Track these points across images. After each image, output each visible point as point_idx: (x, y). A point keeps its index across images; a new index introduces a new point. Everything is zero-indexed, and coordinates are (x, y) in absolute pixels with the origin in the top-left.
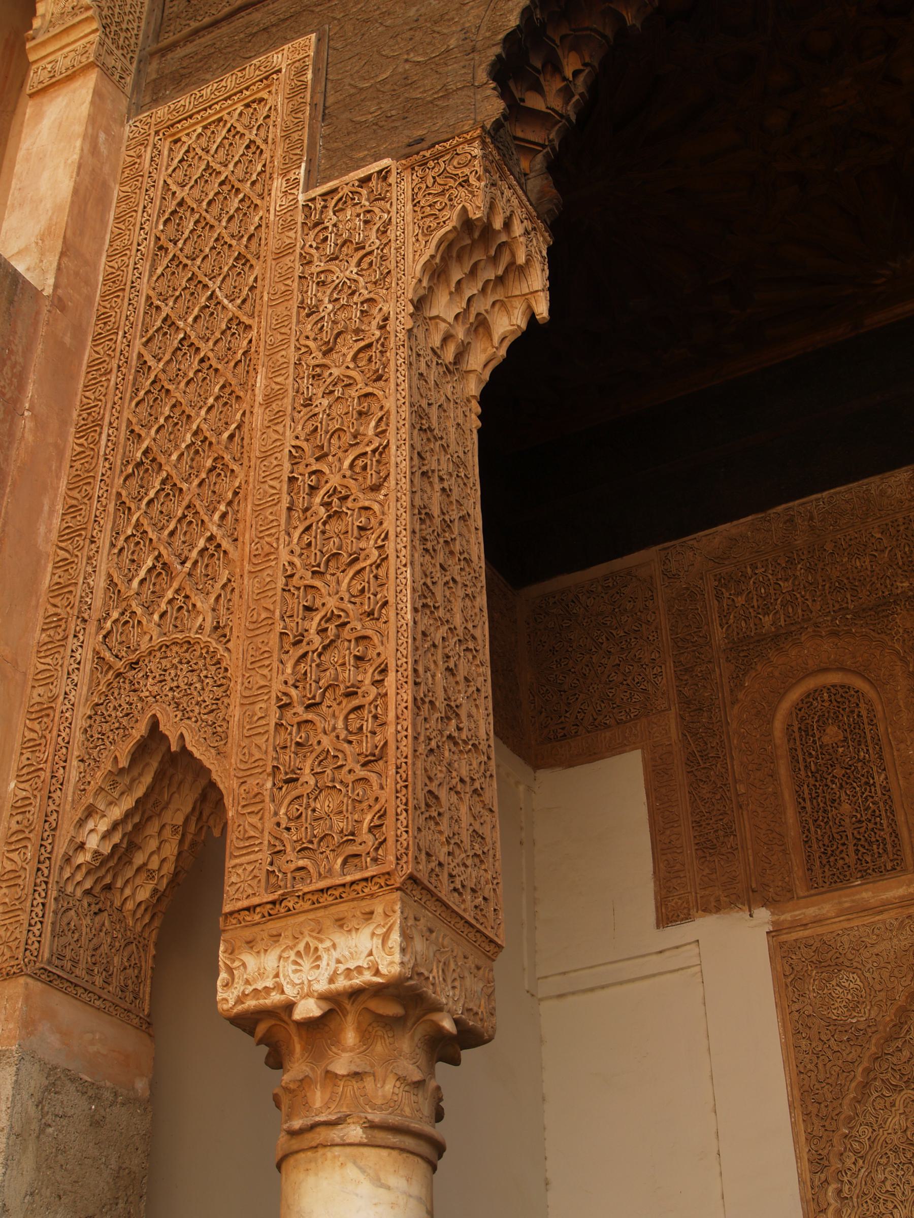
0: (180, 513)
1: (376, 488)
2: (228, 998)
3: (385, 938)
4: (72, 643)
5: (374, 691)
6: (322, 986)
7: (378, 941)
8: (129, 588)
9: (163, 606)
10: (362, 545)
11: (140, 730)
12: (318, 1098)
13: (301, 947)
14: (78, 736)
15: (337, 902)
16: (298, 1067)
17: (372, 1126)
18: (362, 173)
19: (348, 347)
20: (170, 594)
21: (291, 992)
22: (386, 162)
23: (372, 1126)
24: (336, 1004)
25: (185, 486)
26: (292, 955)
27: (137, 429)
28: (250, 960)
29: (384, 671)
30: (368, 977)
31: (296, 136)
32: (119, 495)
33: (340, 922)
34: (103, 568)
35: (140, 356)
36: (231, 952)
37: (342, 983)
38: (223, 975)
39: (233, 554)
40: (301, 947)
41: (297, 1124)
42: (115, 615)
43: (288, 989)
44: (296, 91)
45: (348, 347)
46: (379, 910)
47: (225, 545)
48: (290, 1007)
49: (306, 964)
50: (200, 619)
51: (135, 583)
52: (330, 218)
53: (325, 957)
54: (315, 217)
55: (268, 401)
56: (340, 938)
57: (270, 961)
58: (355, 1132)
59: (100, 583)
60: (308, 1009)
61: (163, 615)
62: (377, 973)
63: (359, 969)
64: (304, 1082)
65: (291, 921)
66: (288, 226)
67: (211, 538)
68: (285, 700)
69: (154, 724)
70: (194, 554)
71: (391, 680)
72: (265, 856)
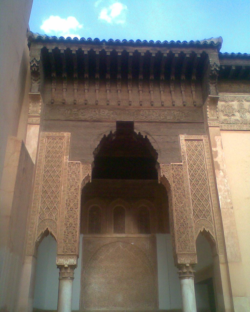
0: (50, 202)
1: (76, 209)
2: (58, 263)
3: (75, 260)
4: (36, 215)
5: (75, 234)
6: (68, 264)
7: (74, 260)
8: (44, 209)
9: (49, 214)
10: (75, 215)
11: (45, 229)
12: (66, 274)
13: (66, 259)
14: (37, 227)
15: (70, 256)
16: (63, 271)
17: (71, 278)
18: (77, 162)
19: (73, 188)
20: (49, 212)
21: (65, 264)
22: (79, 162)
23: (71, 278)
24: (69, 266)
25: (51, 198)
26: (65, 260)
27: (44, 186)
28: (60, 260)
29: (77, 232)
30: (73, 264)
31: (68, 150)
32: (42, 195)
33: (70, 258)
34: (40, 206)
35: (44, 175)
36: (58, 258)
37: (70, 264)
38: (57, 261)
39: (58, 210)
40: (66, 259)
41: (64, 277)
42: (42, 213)
43: (64, 263)
44: (68, 142)
45: (73, 188)
46: (74, 257)
47: (57, 208)
48: (64, 265)
49: (66, 261)
50: (53, 217)
51: (45, 209)
52: (72, 167)
53: (68, 261)
54: (70, 166)
55: (63, 191)
56: (70, 259)
57: (62, 260)
58: (69, 278)
59: (40, 207)
60: (66, 266)
61: (48, 215)
62: (74, 263)
63: (72, 263)
64: (65, 272)
65: (65, 256)
66: (66, 165)
67: (55, 207)
68: (65, 232)
69: (47, 228)
70: (53, 208)
71: (77, 233)
72: (62, 249)
